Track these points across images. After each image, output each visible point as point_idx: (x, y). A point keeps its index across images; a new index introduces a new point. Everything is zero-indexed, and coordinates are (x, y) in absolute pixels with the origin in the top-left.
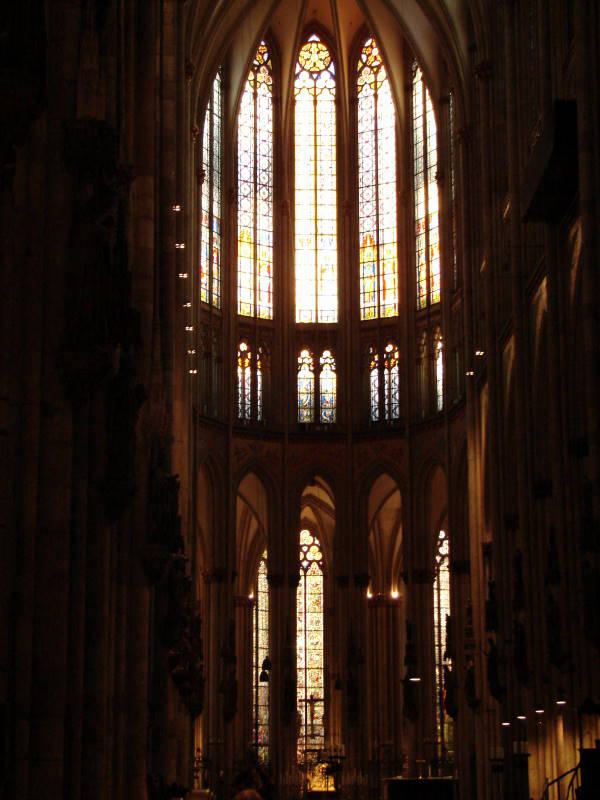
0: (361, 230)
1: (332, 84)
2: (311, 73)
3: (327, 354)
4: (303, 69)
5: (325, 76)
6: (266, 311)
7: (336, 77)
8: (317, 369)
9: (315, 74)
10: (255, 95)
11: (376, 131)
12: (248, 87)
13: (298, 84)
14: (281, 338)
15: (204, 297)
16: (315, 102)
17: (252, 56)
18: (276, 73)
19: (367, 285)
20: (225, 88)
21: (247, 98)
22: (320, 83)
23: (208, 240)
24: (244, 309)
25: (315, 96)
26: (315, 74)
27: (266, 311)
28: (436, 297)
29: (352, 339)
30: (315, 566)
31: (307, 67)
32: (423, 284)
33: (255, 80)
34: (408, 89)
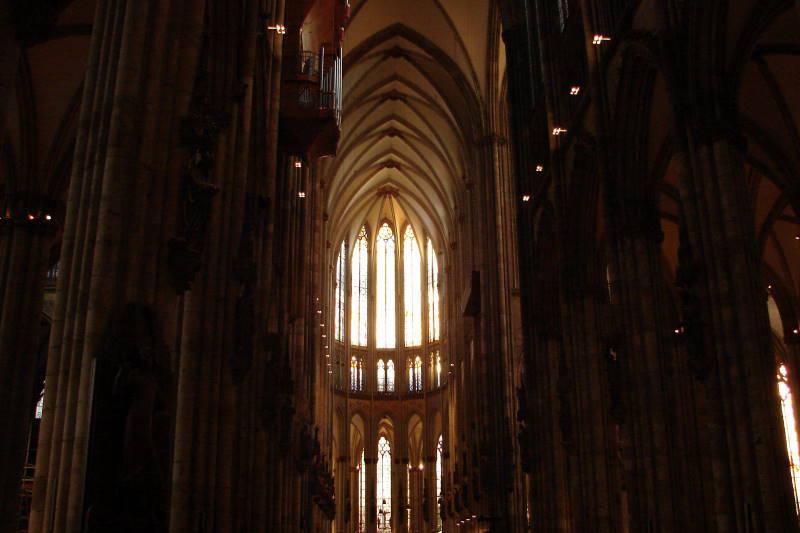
3: (390, 361)
6: (364, 343)
7: (395, 242)
8: (386, 369)
12: (357, 245)
13: (378, 244)
14: (370, 355)
15: (336, 337)
17: (359, 233)
18: (369, 239)
20: (347, 246)
23: (338, 314)
24: (354, 341)
27: (364, 343)
28: (437, 338)
29: (401, 355)
30: (387, 454)
34: (425, 247)
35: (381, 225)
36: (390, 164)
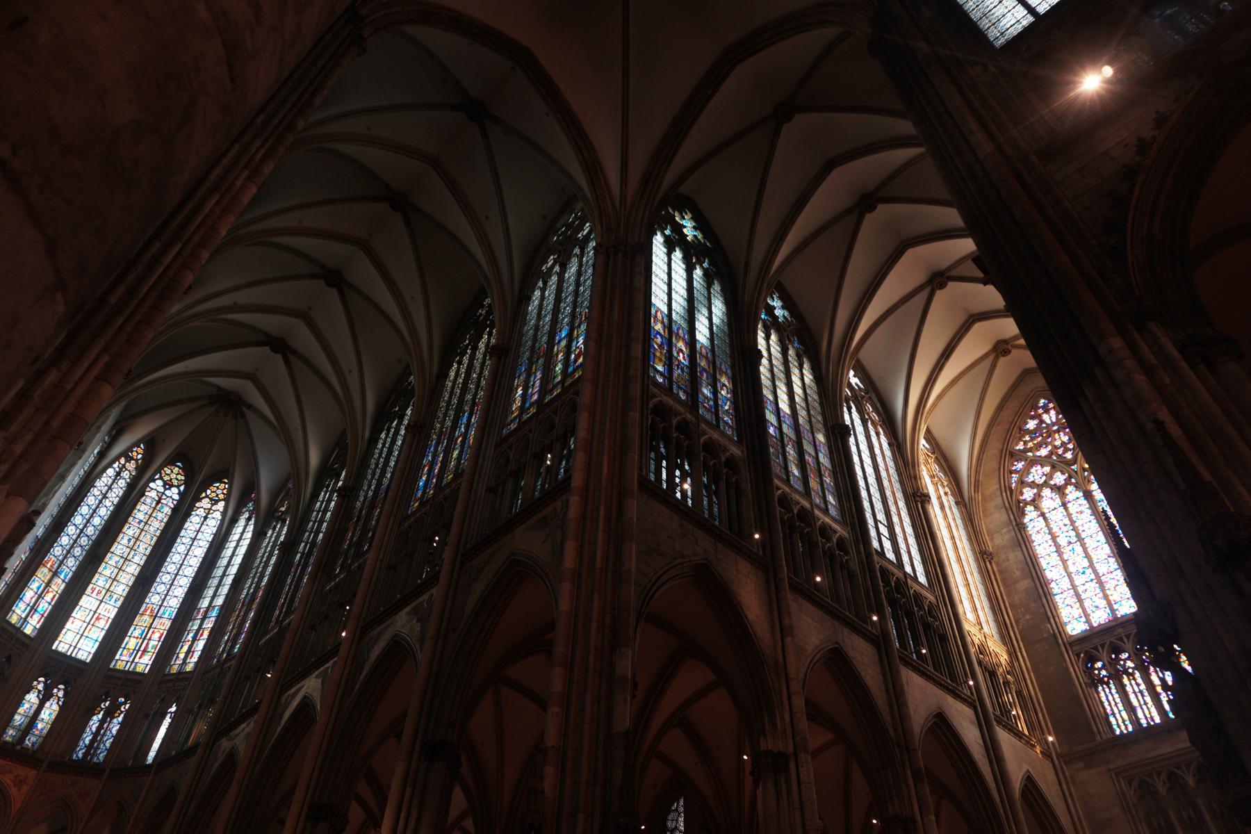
0: (147, 600)
1: (177, 497)
2: (165, 483)
4: (161, 478)
5: (175, 490)
8: (45, 697)
9: (168, 485)
10: (118, 474)
11: (194, 540)
13: (152, 485)
16: (158, 502)
18: (141, 470)
19: (131, 642)
21: (110, 472)
22: (167, 492)
25: (160, 499)
26: (168, 485)
31: (166, 478)
32: (182, 656)
33: (124, 466)
35: (171, 462)
36: (279, 345)
